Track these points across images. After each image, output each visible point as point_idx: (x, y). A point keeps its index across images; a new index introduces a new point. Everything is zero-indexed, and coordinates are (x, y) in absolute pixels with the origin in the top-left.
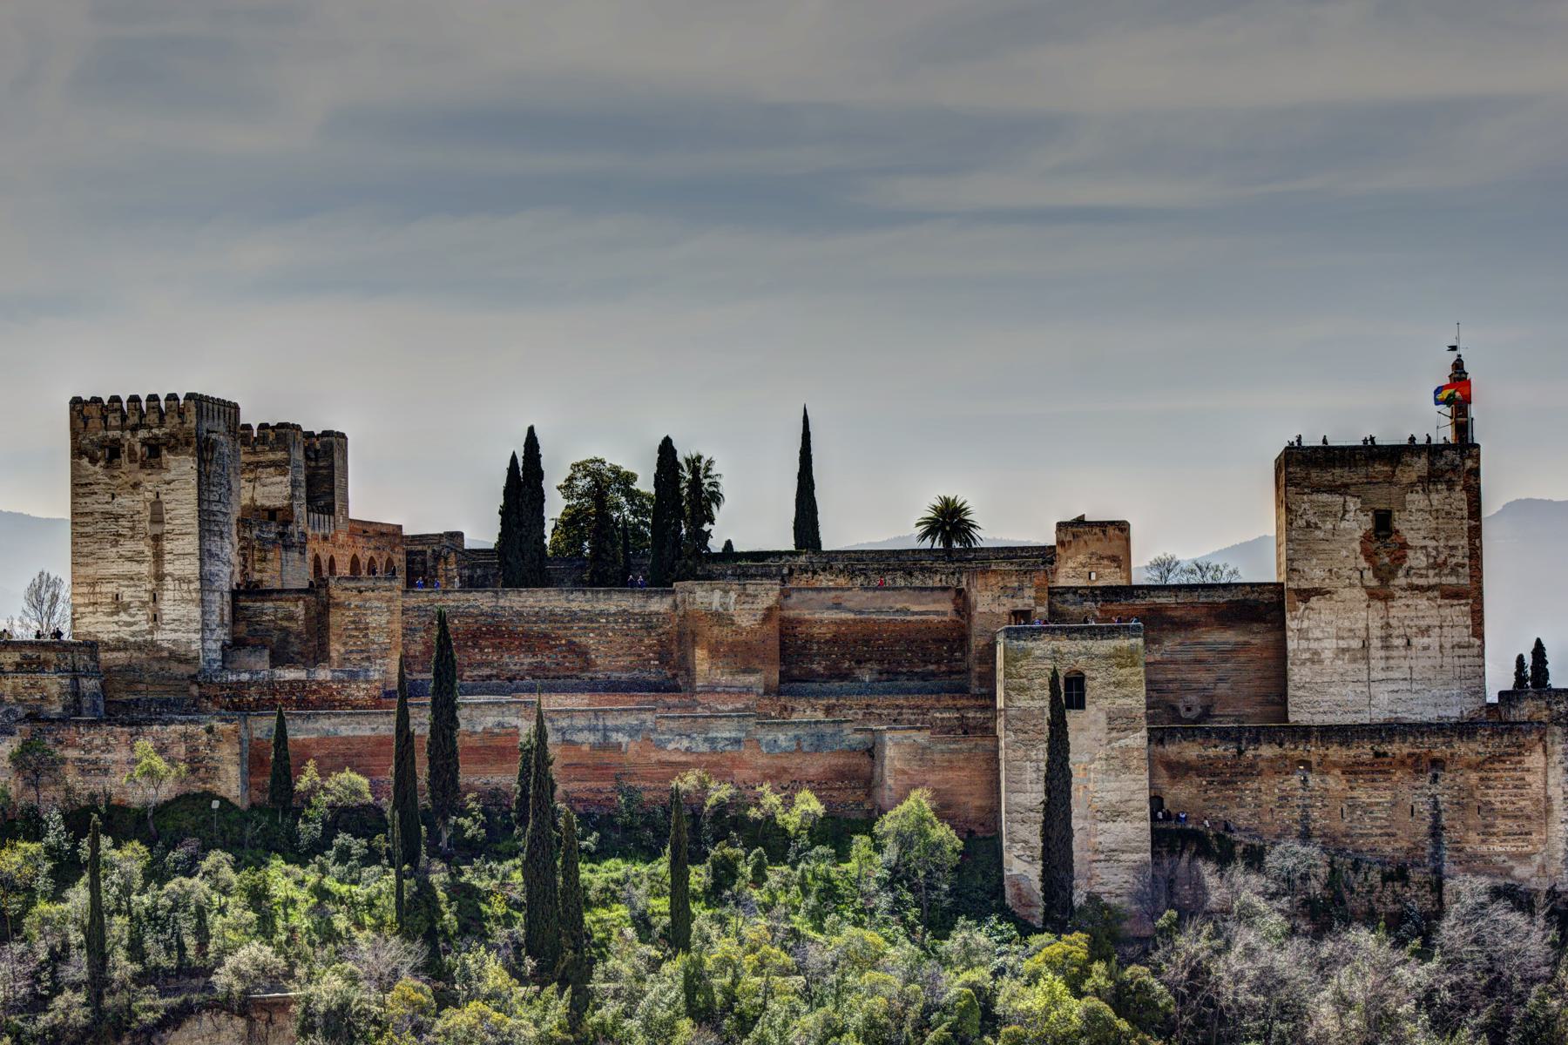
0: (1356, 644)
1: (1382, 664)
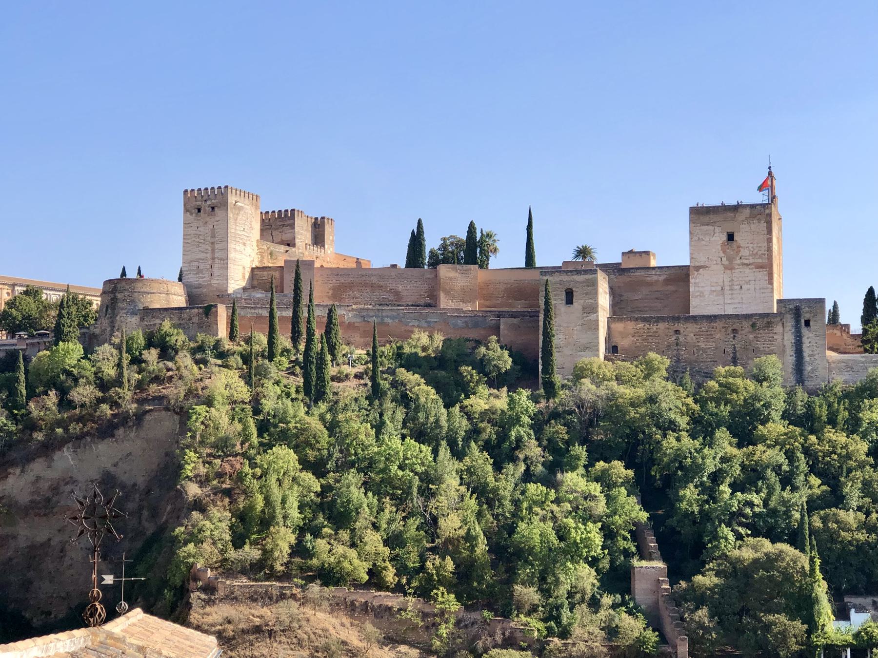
1: (730, 296)
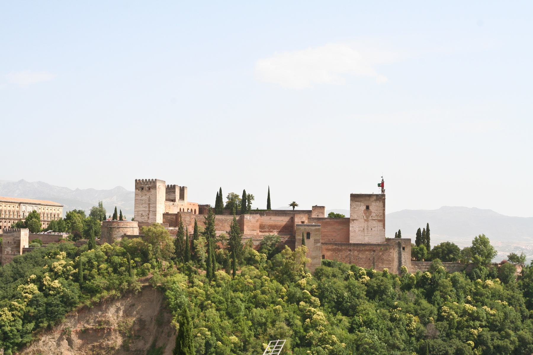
0: (362, 229)
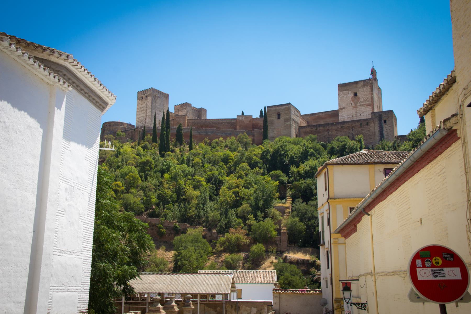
0: (351, 116)
